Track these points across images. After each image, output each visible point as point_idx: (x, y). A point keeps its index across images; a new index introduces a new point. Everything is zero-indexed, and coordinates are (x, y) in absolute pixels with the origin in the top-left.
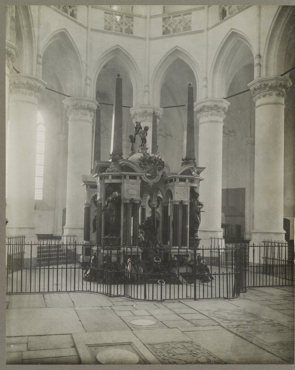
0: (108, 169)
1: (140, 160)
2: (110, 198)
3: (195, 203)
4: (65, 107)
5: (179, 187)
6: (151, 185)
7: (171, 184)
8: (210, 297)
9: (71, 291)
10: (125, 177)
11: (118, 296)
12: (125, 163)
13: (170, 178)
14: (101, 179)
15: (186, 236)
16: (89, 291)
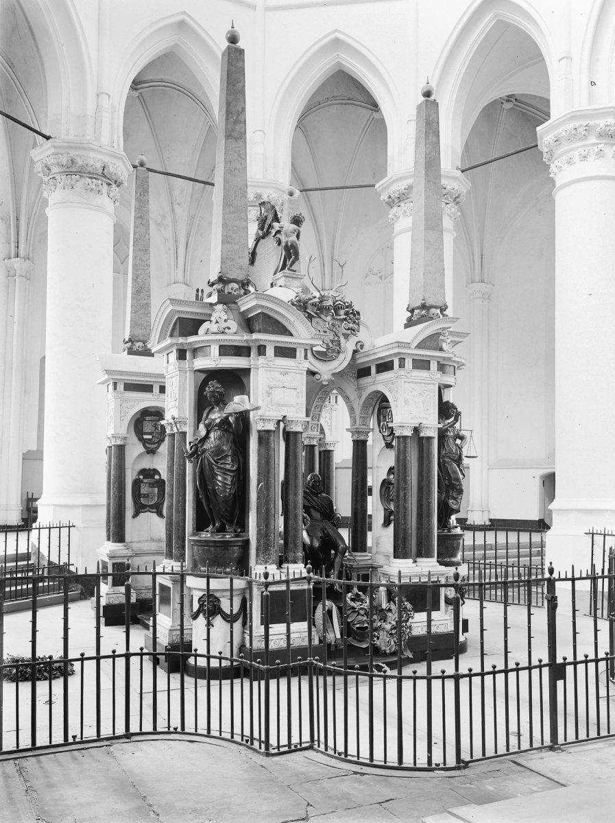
2: (216, 416)
4: (39, 167)
6: (325, 380)
8: (593, 734)
10: (261, 350)
11: (292, 749)
12: (262, 307)
13: (381, 358)
14: (182, 355)
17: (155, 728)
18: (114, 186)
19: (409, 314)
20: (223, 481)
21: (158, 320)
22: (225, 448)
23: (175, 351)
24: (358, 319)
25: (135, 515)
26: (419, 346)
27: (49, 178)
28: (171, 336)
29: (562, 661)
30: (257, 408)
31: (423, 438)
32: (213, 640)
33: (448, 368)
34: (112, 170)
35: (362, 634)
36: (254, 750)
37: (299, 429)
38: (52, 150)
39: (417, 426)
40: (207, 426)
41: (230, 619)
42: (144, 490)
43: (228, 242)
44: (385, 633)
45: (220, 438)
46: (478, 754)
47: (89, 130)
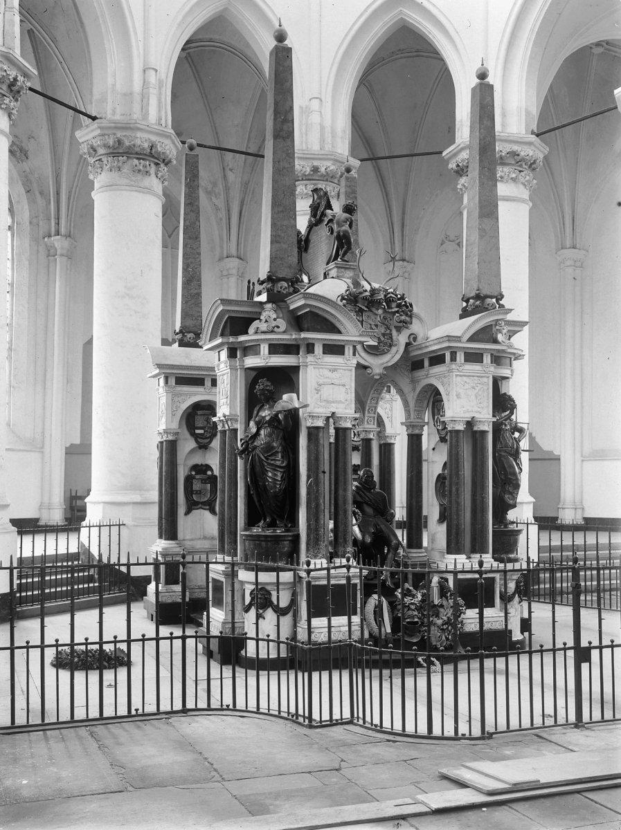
0: (255, 324)
1: (343, 298)
2: (266, 413)
3: (506, 425)
4: (84, 149)
5: (465, 378)
6: (376, 375)
7: (438, 369)
9: (173, 712)
11: (332, 723)
13: (433, 351)
14: (232, 354)
15: (485, 525)
16: (228, 709)
17: (209, 704)
18: (162, 165)
19: (465, 304)
20: (274, 477)
21: (209, 319)
22: (275, 444)
23: (226, 349)
24: (411, 311)
25: (187, 513)
26: (471, 340)
27: (95, 159)
28: (222, 335)
29: (588, 645)
30: (306, 406)
31: (476, 432)
32: (264, 632)
33: (503, 361)
34: (159, 149)
35: (413, 628)
36: (299, 724)
37: (349, 425)
38: (98, 132)
39: (470, 420)
40: (257, 424)
41: (281, 612)
42: (197, 486)
43: (277, 242)
44: (436, 628)
45: (270, 435)
46: (502, 725)
47: (136, 107)
